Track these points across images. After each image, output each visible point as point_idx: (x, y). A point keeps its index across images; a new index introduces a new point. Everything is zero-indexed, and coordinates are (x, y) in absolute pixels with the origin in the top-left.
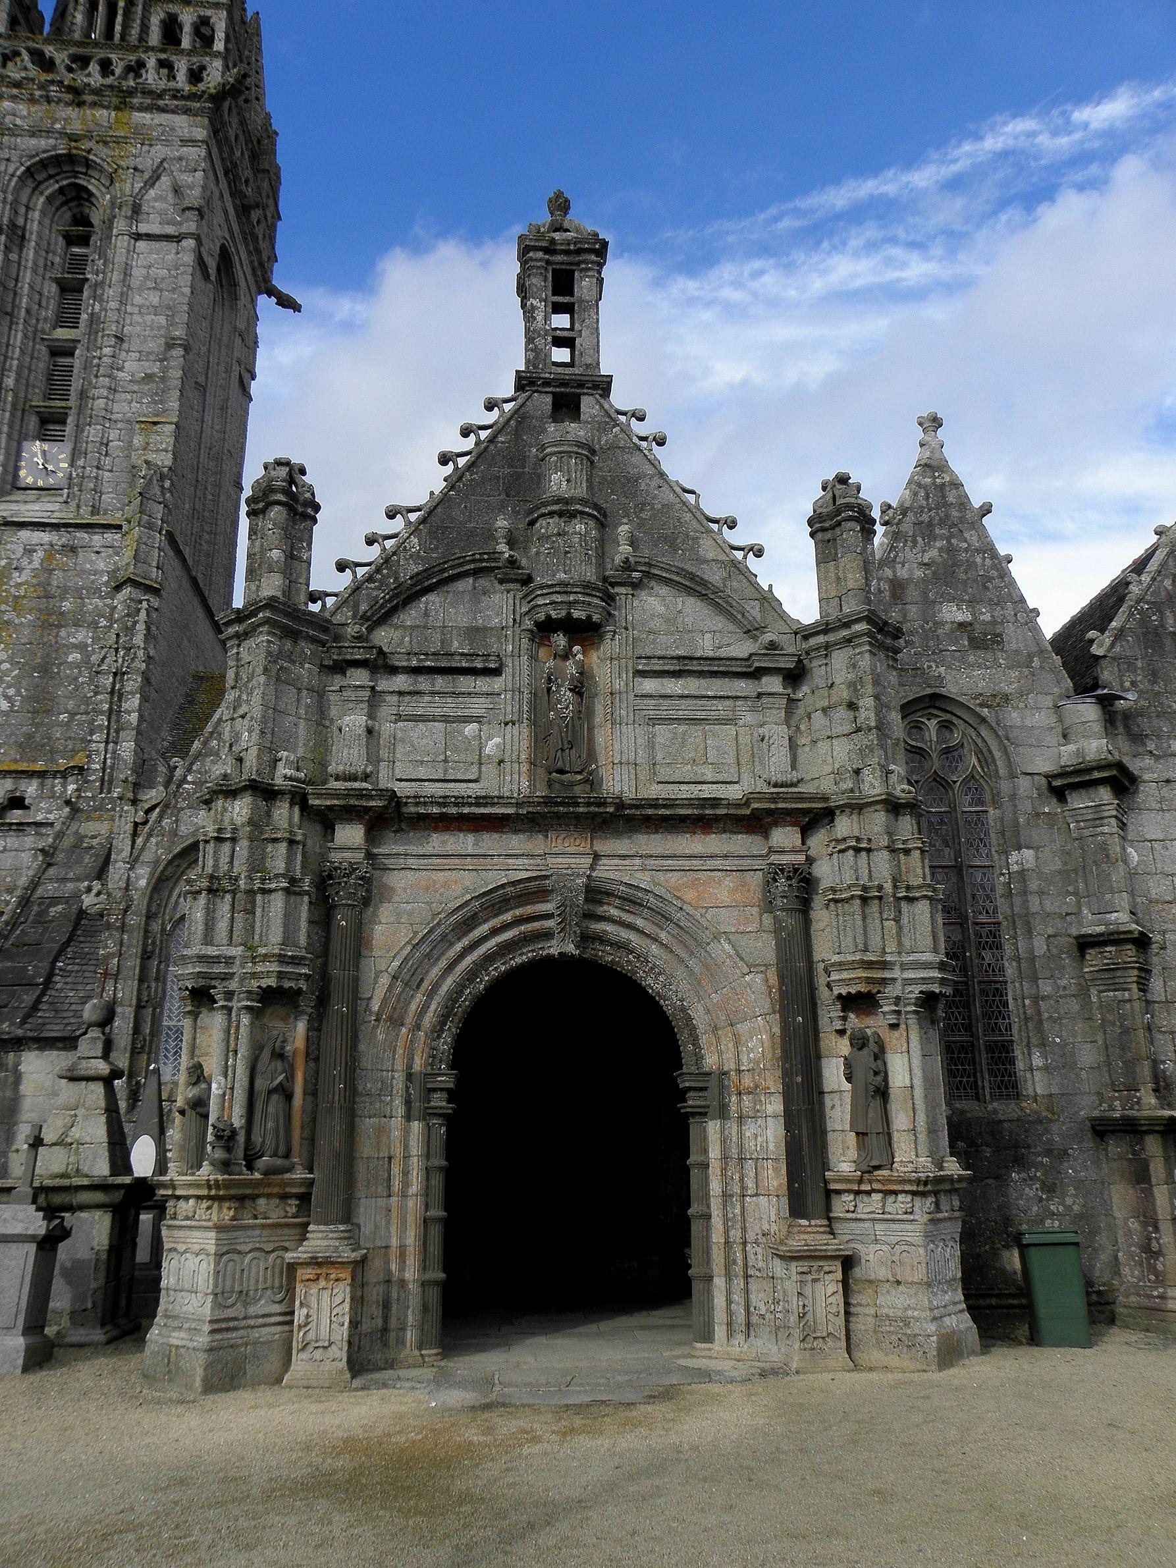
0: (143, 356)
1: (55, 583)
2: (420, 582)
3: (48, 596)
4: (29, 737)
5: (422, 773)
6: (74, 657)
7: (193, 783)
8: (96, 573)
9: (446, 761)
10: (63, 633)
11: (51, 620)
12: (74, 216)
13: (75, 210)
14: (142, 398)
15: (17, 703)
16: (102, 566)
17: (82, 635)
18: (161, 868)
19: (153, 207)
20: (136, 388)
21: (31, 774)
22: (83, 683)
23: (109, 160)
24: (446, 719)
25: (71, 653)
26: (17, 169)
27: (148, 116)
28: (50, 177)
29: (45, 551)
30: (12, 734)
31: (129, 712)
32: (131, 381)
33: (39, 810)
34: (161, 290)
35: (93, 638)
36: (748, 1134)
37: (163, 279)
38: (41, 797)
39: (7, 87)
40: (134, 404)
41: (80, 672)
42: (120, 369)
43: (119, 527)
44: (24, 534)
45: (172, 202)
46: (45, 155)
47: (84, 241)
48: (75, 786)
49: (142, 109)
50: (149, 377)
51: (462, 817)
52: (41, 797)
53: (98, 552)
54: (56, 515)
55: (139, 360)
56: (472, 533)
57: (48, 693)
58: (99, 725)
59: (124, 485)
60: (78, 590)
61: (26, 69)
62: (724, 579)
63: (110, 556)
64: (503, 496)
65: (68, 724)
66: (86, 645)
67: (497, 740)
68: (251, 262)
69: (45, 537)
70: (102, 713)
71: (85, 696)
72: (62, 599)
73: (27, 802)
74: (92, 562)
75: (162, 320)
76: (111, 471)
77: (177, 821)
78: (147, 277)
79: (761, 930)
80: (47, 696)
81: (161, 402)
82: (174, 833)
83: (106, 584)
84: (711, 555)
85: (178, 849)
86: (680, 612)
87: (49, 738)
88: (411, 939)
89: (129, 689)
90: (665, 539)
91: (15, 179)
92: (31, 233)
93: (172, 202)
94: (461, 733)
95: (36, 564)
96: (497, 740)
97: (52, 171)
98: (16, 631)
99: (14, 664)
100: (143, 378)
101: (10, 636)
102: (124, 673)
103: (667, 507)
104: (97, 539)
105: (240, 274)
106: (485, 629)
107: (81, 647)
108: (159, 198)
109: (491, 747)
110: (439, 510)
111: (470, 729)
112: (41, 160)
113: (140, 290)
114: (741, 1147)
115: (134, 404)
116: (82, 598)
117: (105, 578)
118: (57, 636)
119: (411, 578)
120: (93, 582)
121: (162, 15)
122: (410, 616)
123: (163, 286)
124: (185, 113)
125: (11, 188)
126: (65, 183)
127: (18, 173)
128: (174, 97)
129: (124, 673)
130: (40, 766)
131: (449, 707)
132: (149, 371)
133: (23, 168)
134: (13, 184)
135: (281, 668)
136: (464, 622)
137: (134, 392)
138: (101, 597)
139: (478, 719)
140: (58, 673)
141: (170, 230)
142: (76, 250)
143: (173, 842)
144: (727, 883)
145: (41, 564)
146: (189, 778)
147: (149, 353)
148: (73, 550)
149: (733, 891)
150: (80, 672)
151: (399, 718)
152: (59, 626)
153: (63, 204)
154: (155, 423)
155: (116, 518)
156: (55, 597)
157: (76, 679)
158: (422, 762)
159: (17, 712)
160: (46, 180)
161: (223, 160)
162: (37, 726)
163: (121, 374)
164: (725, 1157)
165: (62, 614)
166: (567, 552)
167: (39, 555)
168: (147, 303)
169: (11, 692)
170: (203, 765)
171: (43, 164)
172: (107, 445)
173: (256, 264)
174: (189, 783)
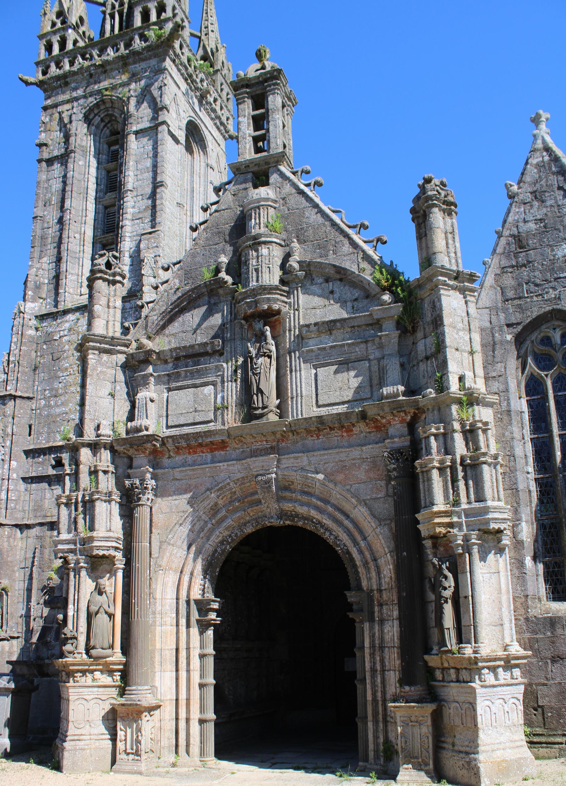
2: (177, 306)
12: (110, 131)
13: (110, 128)
24: (195, 386)
27: (137, 66)
28: (96, 115)
36: (386, 631)
47: (116, 142)
49: (135, 63)
68: (215, 124)
79: (387, 495)
88: (178, 521)
97: (96, 112)
105: (206, 133)
114: (382, 639)
119: (171, 304)
124: (155, 57)
128: (149, 51)
135: (100, 372)
144: (364, 467)
149: (367, 471)
153: (104, 127)
158: (182, 414)
160: (94, 117)
161: (182, 75)
164: (373, 646)
171: (91, 110)
173: (218, 124)
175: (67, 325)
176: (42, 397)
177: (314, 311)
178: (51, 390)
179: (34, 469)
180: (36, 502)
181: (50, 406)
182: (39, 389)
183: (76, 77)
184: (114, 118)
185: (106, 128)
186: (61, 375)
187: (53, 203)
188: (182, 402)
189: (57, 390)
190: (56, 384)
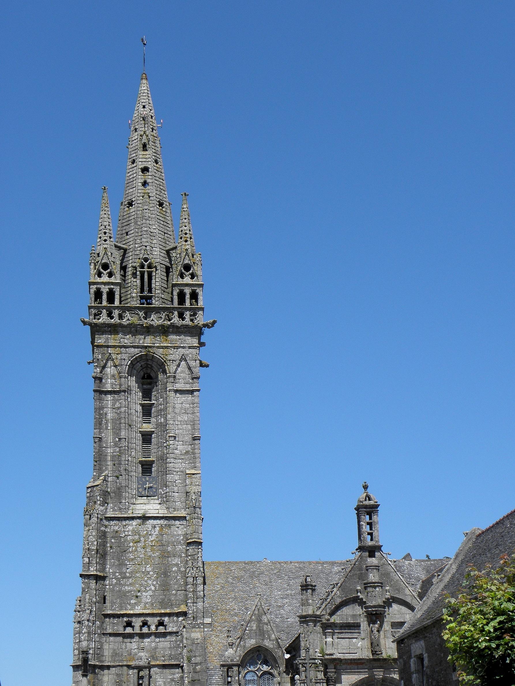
0: (184, 443)
1: (164, 540)
3: (163, 545)
4: (163, 600)
5: (344, 651)
6: (175, 569)
7: (248, 630)
8: (178, 535)
9: (349, 648)
10: (170, 559)
11: (165, 555)
14: (186, 461)
15: (157, 587)
16: (180, 533)
17: (176, 561)
18: (242, 658)
19: (180, 376)
20: (183, 458)
21: (165, 615)
22: (179, 579)
23: (162, 356)
25: (174, 567)
26: (128, 362)
28: (138, 362)
29: (159, 527)
30: (157, 599)
31: (200, 592)
32: (181, 454)
33: (169, 627)
34: (188, 414)
35: (180, 561)
37: (188, 409)
38: (169, 622)
39: (121, 328)
40: (183, 464)
41: (177, 575)
42: (176, 449)
43: (185, 517)
44: (151, 522)
45: (187, 373)
46: (137, 355)
48: (182, 618)
50: (187, 452)
51: (355, 663)
52: (169, 622)
53: (178, 527)
54: (160, 511)
55: (183, 445)
56: (351, 590)
57: (167, 583)
58: (190, 596)
59: (183, 498)
60: (173, 542)
61: (128, 320)
62: (411, 600)
63: (183, 529)
64: (358, 579)
65: (176, 594)
66: (178, 564)
67: (361, 643)
69: (158, 522)
70: (190, 592)
71: (180, 584)
72: (168, 546)
73: (165, 624)
74: (176, 531)
75: (189, 427)
76: (177, 493)
77: (245, 643)
78: (181, 408)
80: (168, 584)
81: (193, 463)
82: (244, 646)
83: (182, 539)
84: (408, 593)
85: (246, 651)
86: (401, 609)
87: (170, 600)
89: (198, 583)
90: (397, 589)
91: (127, 366)
92: (133, 387)
93: (187, 373)
94: (352, 642)
95: (157, 533)
96: (361, 643)
98: (153, 559)
99: (154, 572)
100: (185, 453)
101: (152, 561)
102: (197, 577)
103: (397, 580)
104: (177, 522)
106: (356, 615)
107: (177, 565)
108: (182, 372)
109: (359, 644)
110: (343, 584)
111: (354, 640)
112: (136, 357)
113: (180, 415)
115: (183, 464)
116: (174, 546)
117: (182, 538)
118: (168, 561)
120: (178, 539)
121: (178, 291)
122: (339, 613)
123: (188, 412)
125: (126, 371)
126: (143, 363)
127: (128, 364)
128: (186, 328)
129: (197, 577)
130: (168, 611)
131: (349, 636)
132: (187, 450)
133: (130, 362)
134: (127, 369)
136: (351, 613)
137: (182, 459)
138: (181, 545)
139: (356, 638)
140: (170, 575)
141: (188, 387)
142: (145, 387)
143: (244, 650)
145: (159, 532)
146: (247, 629)
147: (186, 442)
148: (169, 526)
150: (177, 575)
151: (338, 638)
152: (168, 557)
154: (193, 474)
155: (182, 513)
156: (165, 546)
157: (176, 577)
159: (158, 590)
160: (136, 363)
162: (165, 595)
163: (176, 451)
165: (169, 552)
166: (375, 596)
167: (158, 529)
168: (183, 420)
169: (155, 583)
170: (251, 624)
172: (175, 482)
174: (247, 630)
175: (130, 528)
176: (114, 577)
177: (395, 615)
178: (120, 573)
179: (111, 627)
180: (114, 650)
181: (120, 584)
182: (111, 571)
183: (124, 329)
184: (150, 366)
185: (142, 371)
186: (128, 563)
187: (109, 428)
188: (344, 644)
189: (125, 573)
190: (124, 570)
